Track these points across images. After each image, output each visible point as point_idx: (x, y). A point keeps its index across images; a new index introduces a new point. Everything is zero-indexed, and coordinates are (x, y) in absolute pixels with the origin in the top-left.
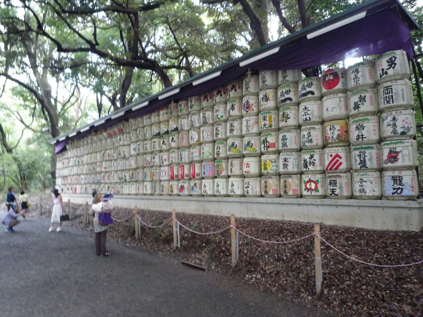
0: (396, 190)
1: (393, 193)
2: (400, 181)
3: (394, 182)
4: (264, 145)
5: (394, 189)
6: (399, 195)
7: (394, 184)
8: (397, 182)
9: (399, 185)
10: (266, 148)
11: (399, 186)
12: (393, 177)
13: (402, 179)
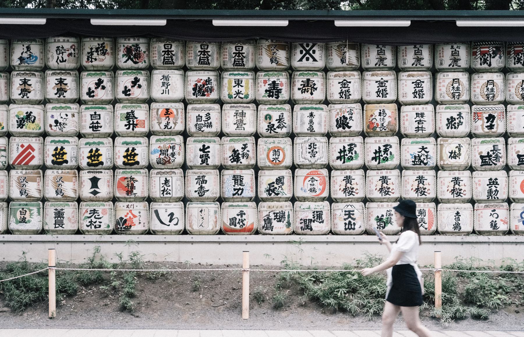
0: (237, 191)
1: (234, 195)
2: (241, 181)
3: (235, 182)
4: (129, 122)
5: (235, 190)
9: (240, 185)
10: (131, 126)
12: (234, 176)
13: (243, 179)
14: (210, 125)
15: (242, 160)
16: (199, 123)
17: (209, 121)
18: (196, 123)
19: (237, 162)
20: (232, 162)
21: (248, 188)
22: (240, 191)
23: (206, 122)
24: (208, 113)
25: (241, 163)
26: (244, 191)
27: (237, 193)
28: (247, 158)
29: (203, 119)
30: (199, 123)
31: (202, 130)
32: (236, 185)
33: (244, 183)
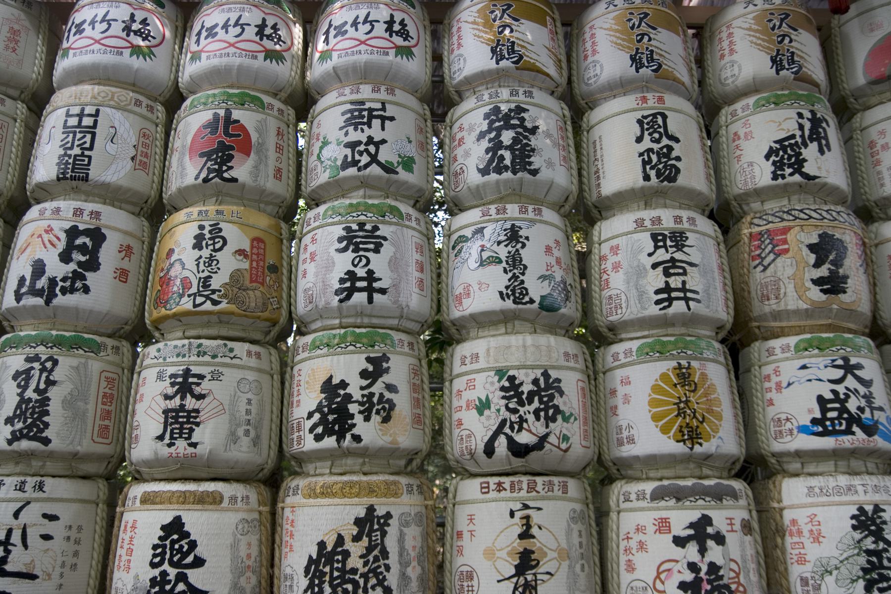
15: (361, 427)
19: (341, 437)
20: (318, 438)
25: (357, 438)
28: (386, 420)
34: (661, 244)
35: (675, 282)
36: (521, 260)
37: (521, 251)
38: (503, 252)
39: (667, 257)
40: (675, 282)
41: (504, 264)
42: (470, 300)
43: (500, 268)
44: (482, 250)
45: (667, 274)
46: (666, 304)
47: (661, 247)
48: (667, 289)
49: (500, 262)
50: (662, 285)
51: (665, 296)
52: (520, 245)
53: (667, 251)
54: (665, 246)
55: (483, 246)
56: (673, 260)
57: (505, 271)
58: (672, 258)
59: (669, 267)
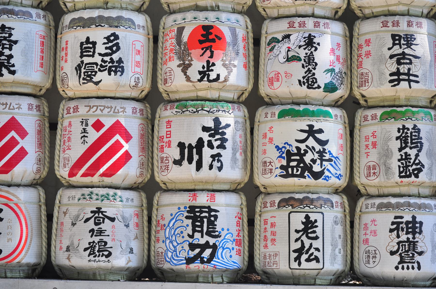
0: (197, 251)
1: (190, 261)
3: (194, 226)
5: (192, 247)
6: (206, 265)
7: (194, 231)
8: (202, 226)
9: (209, 234)
11: (206, 238)
12: (192, 209)
14: (117, 68)
16: (87, 60)
17: (115, 57)
18: (79, 61)
21: (229, 245)
22: (207, 253)
23: (107, 59)
24: (113, 34)
26: (219, 252)
27: (198, 256)
29: (97, 51)
30: (87, 60)
31: (95, 79)
32: (197, 235)
33: (218, 228)
34: (397, 42)
35: (404, 69)
36: (314, 60)
37: (314, 53)
38: (302, 53)
39: (400, 51)
40: (404, 69)
41: (303, 62)
42: (279, 83)
43: (300, 64)
44: (288, 51)
45: (399, 63)
46: (396, 83)
47: (397, 44)
48: (398, 73)
49: (300, 60)
50: (394, 70)
51: (396, 77)
52: (314, 49)
53: (401, 48)
54: (400, 44)
55: (289, 48)
56: (404, 54)
57: (303, 66)
58: (403, 52)
59: (401, 59)
